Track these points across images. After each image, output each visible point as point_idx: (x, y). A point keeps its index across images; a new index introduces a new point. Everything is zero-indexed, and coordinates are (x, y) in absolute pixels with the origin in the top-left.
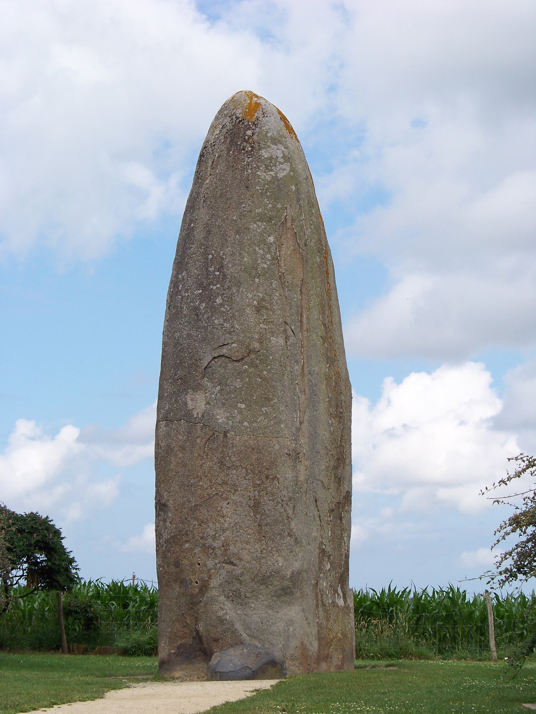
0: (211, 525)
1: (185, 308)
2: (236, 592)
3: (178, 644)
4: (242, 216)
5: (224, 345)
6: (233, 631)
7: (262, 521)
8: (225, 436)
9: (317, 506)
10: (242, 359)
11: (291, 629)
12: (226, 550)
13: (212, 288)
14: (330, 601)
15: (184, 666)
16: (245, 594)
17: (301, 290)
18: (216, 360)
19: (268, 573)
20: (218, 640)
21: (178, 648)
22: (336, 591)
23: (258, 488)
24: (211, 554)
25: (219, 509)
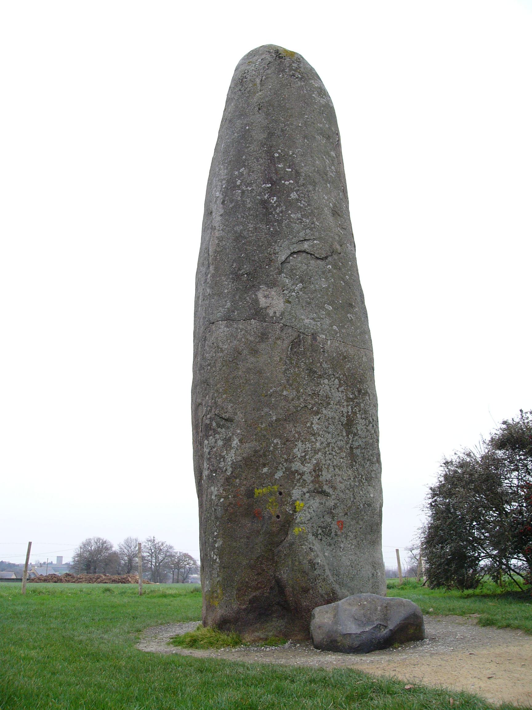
1: (248, 201)
2: (326, 528)
3: (251, 597)
4: (305, 123)
5: (305, 240)
6: (324, 579)
7: (354, 443)
10: (326, 258)
12: (318, 476)
13: (284, 184)
15: (258, 625)
16: (336, 532)
18: (295, 256)
19: (361, 505)
20: (309, 590)
21: (251, 602)
24: (298, 480)
25: (308, 425)
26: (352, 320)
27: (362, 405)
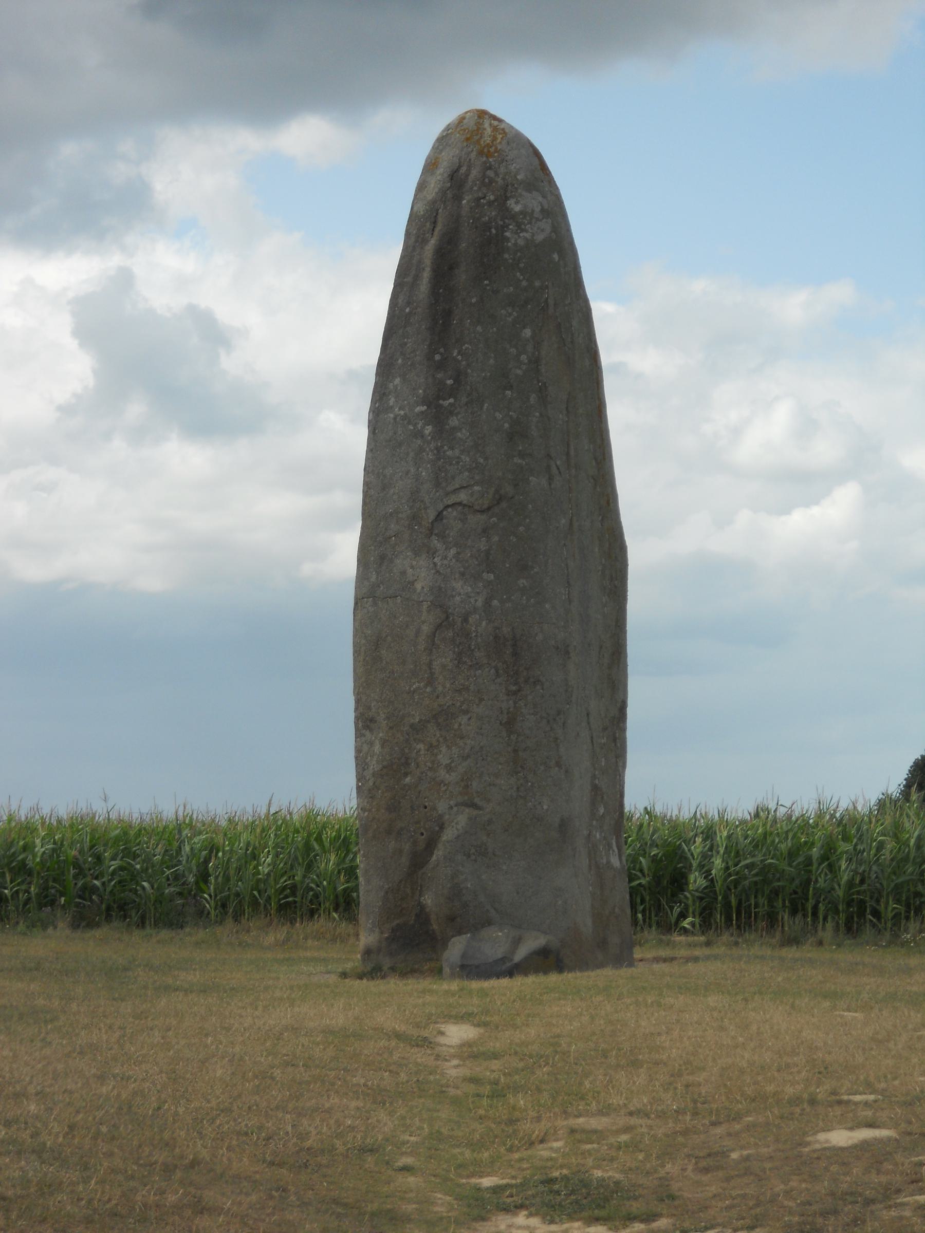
0: (444, 749)
8: (466, 620)
9: (589, 723)
10: (489, 508)
11: (560, 902)
12: (467, 786)
14: (605, 861)
17: (567, 408)
21: (393, 930)
22: (610, 846)
27: (530, 697)
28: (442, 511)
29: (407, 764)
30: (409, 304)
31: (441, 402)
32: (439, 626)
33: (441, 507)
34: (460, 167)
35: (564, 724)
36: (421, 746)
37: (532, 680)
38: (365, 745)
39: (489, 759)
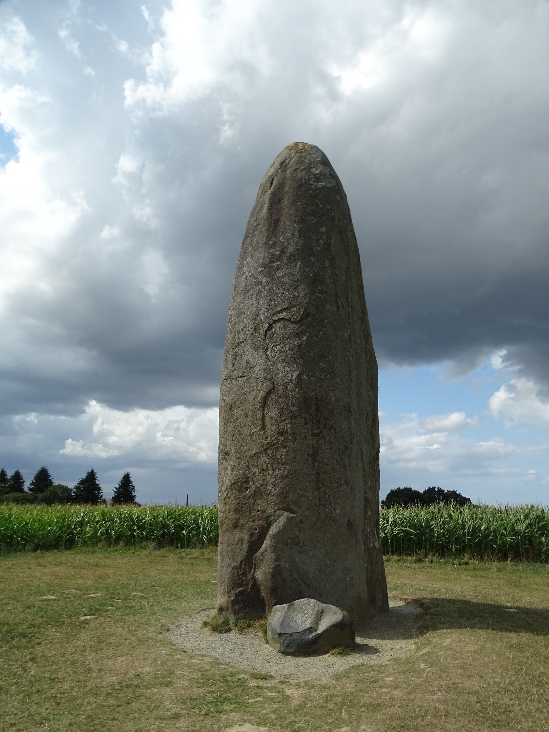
0: (271, 472)
9: (362, 458)
10: (300, 321)
12: (286, 497)
14: (372, 545)
21: (237, 595)
22: (374, 536)
23: (316, 437)
26: (323, 368)
28: (272, 324)
29: (247, 482)
30: (256, 221)
31: (272, 264)
32: (269, 393)
33: (271, 321)
34: (286, 160)
35: (349, 456)
36: (256, 470)
37: (328, 426)
38: (223, 470)
39: (300, 478)
